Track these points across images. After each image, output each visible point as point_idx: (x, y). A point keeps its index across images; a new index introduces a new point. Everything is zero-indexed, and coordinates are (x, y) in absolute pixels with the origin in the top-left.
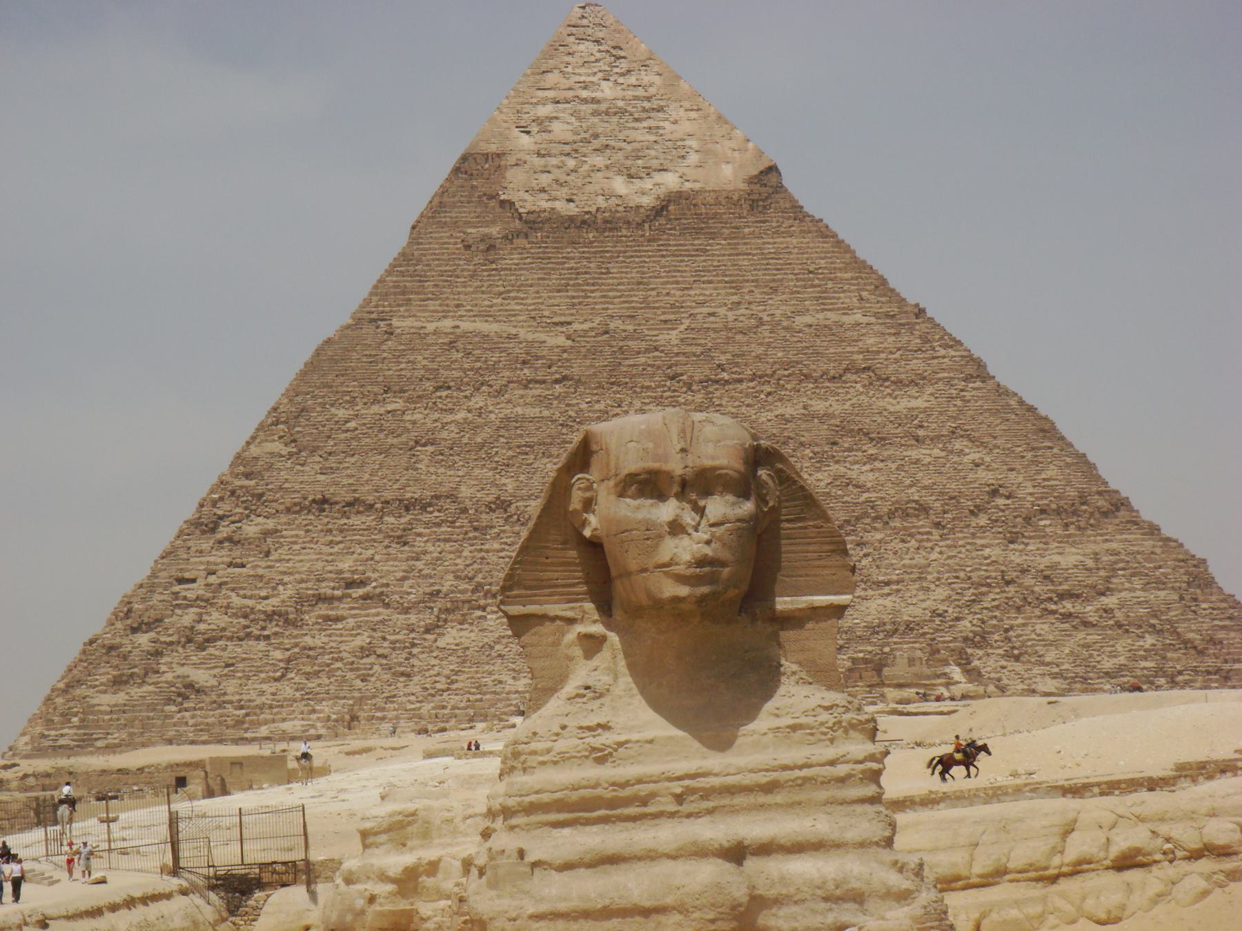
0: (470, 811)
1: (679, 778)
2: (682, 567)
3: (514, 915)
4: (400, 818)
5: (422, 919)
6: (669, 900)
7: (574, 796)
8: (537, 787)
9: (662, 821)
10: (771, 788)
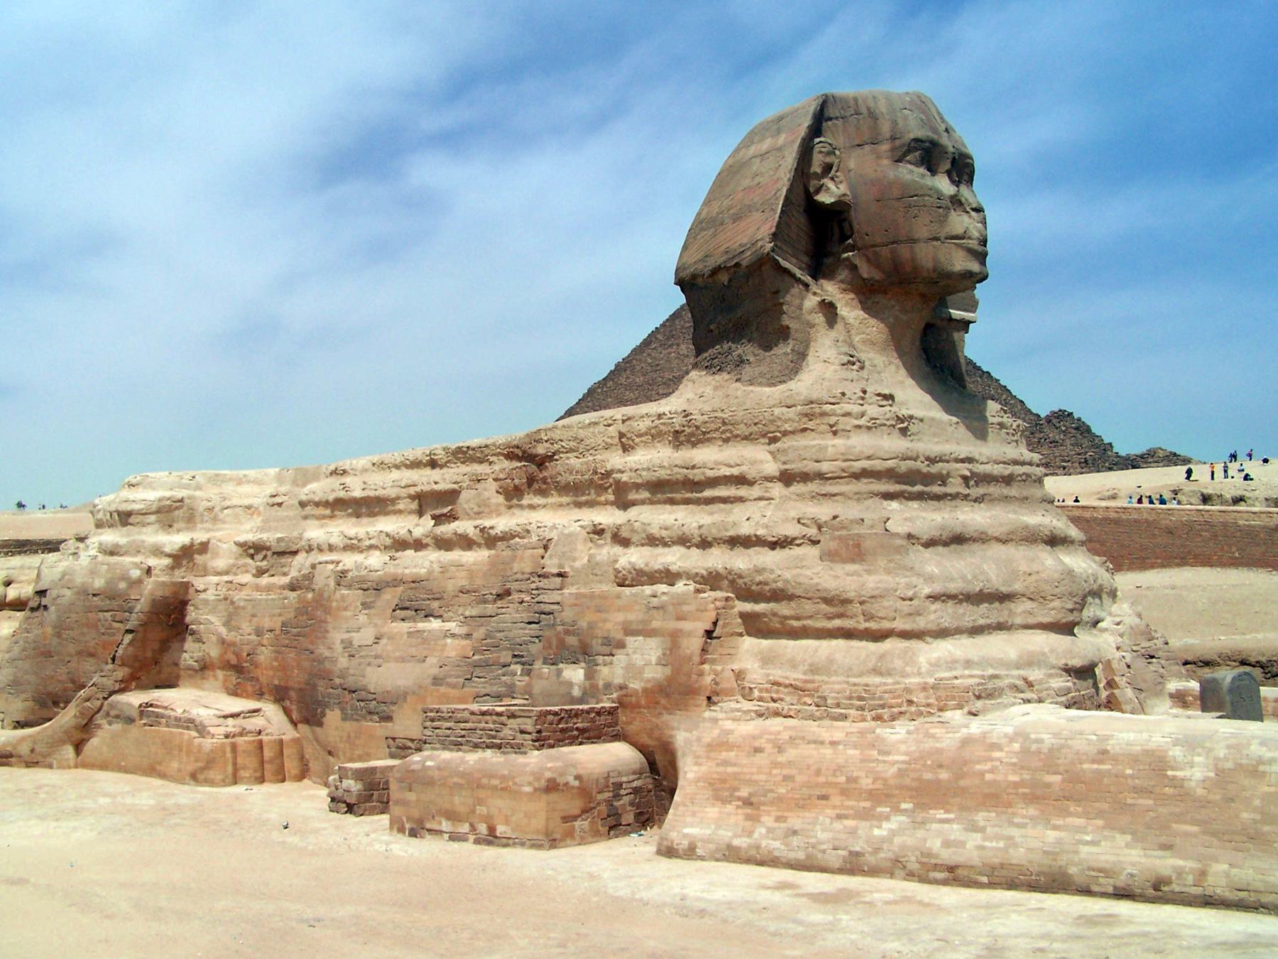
0: (227, 503)
1: (963, 461)
2: (975, 242)
3: (910, 593)
4: (168, 503)
5: (197, 591)
6: (1018, 587)
7: (904, 466)
8: (871, 452)
9: (958, 502)
10: (1008, 480)
